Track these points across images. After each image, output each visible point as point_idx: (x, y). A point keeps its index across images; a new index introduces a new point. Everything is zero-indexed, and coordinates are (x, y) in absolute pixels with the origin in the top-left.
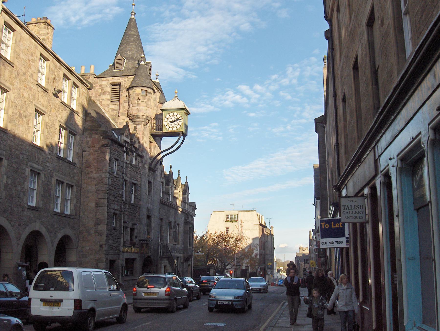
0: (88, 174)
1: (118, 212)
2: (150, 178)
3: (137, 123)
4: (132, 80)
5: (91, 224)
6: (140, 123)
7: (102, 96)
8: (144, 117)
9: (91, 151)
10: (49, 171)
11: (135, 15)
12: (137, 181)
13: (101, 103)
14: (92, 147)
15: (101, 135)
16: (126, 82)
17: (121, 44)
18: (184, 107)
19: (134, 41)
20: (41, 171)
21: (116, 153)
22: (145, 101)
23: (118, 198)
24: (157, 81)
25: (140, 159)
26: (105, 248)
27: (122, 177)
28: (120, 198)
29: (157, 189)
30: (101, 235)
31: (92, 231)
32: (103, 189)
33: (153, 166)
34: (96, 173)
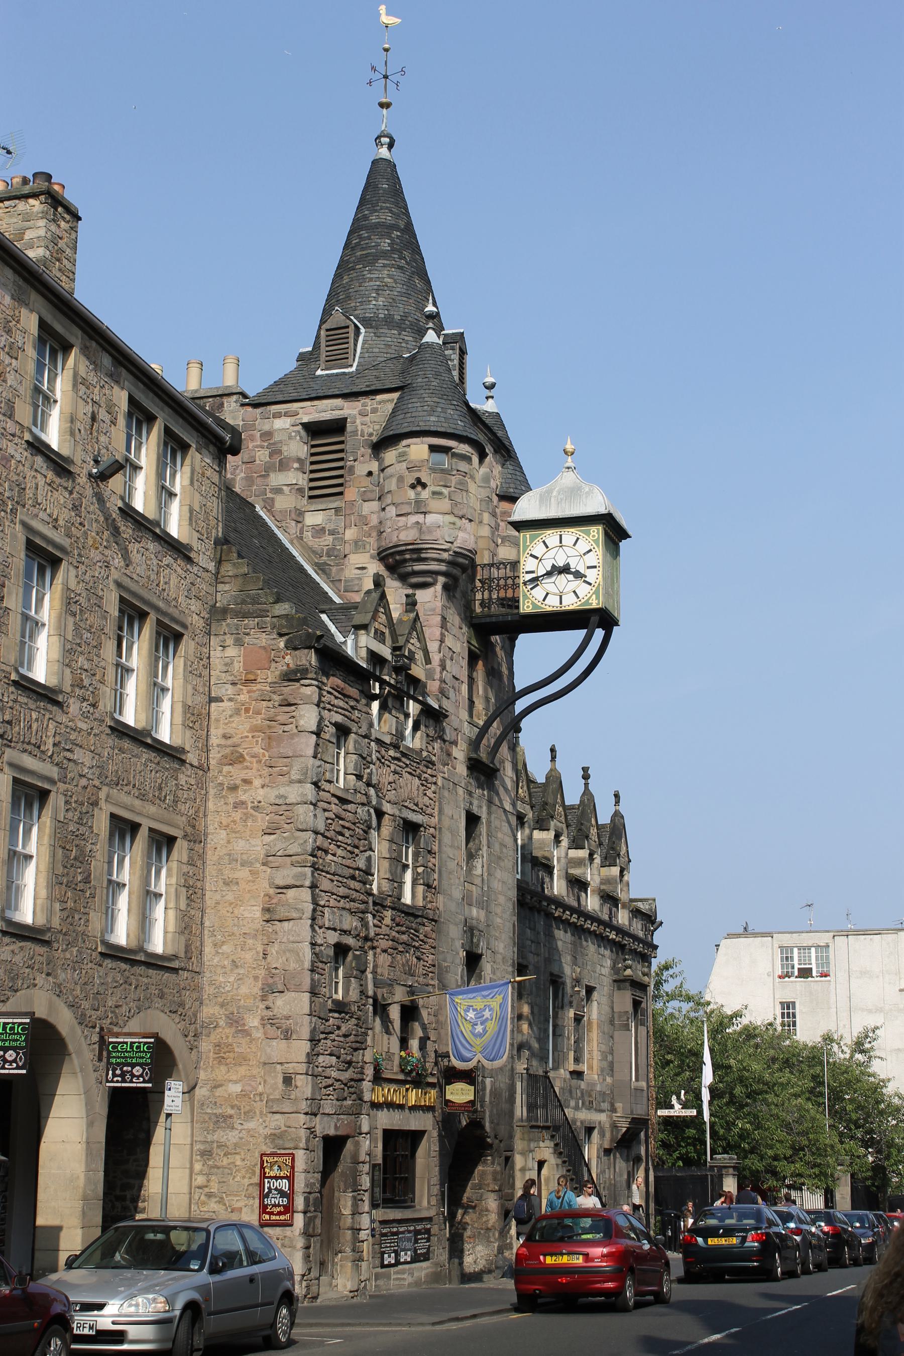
0: (234, 788)
1: (350, 941)
2: (475, 802)
3: (414, 580)
4: (390, 407)
5: (250, 989)
6: (429, 580)
7: (272, 475)
9: (244, 697)
10: (83, 782)
11: (391, 146)
12: (422, 812)
13: (269, 505)
14: (248, 681)
15: (281, 635)
16: (366, 418)
17: (344, 267)
18: (603, 511)
19: (393, 250)
20: (52, 782)
21: (341, 703)
22: (445, 491)
24: (490, 406)
26: (304, 1086)
29: (503, 845)
30: (287, 1035)
31: (253, 1022)
32: (294, 849)
33: (483, 755)
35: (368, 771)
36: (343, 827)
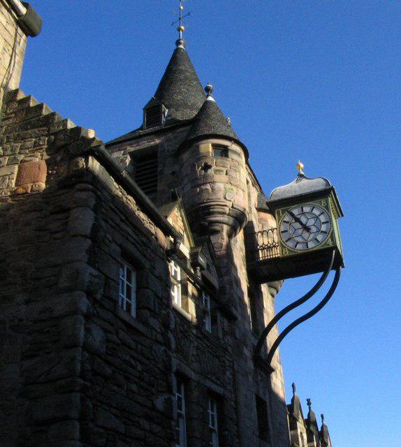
8: (227, 210)
12: (223, 386)
21: (129, 230)
23: (146, 425)
25: (226, 323)
27: (160, 338)
28: (156, 428)
34: (27, 302)
35: (164, 312)
36: (133, 358)
